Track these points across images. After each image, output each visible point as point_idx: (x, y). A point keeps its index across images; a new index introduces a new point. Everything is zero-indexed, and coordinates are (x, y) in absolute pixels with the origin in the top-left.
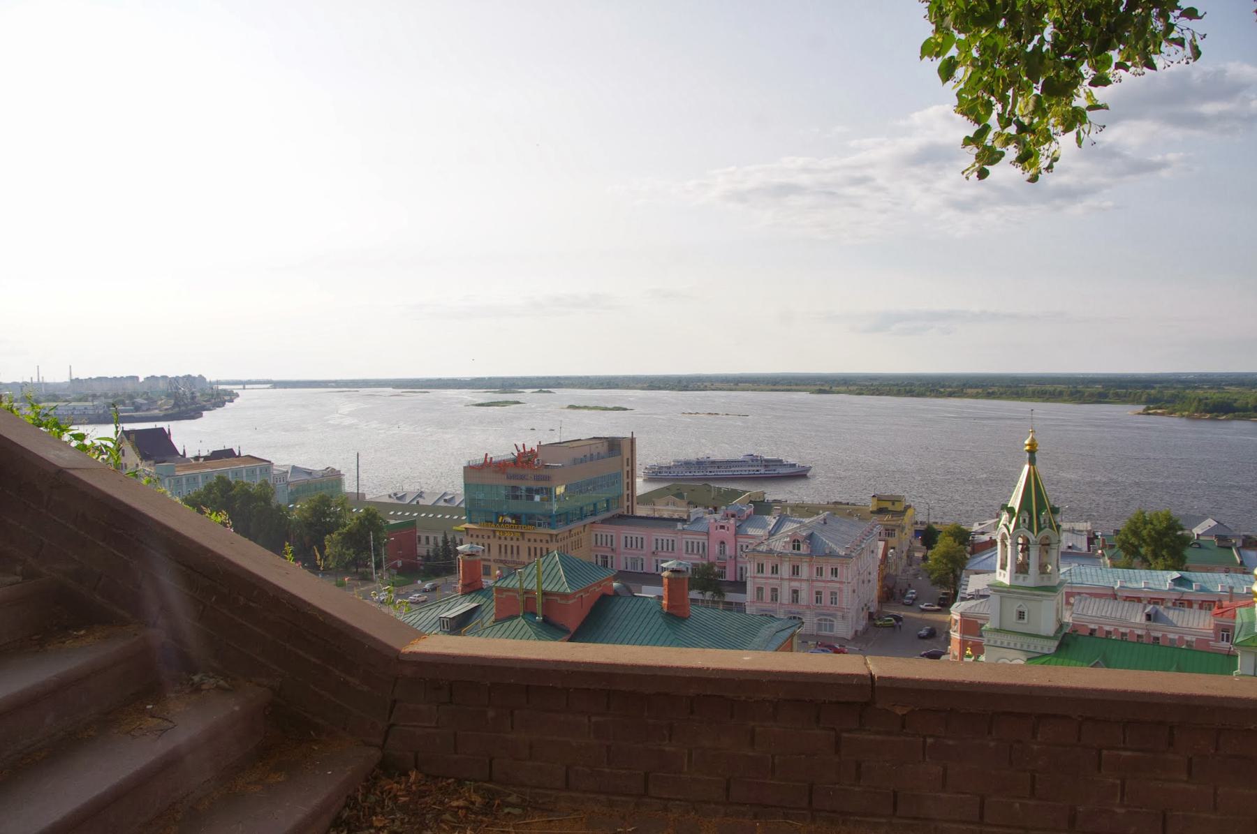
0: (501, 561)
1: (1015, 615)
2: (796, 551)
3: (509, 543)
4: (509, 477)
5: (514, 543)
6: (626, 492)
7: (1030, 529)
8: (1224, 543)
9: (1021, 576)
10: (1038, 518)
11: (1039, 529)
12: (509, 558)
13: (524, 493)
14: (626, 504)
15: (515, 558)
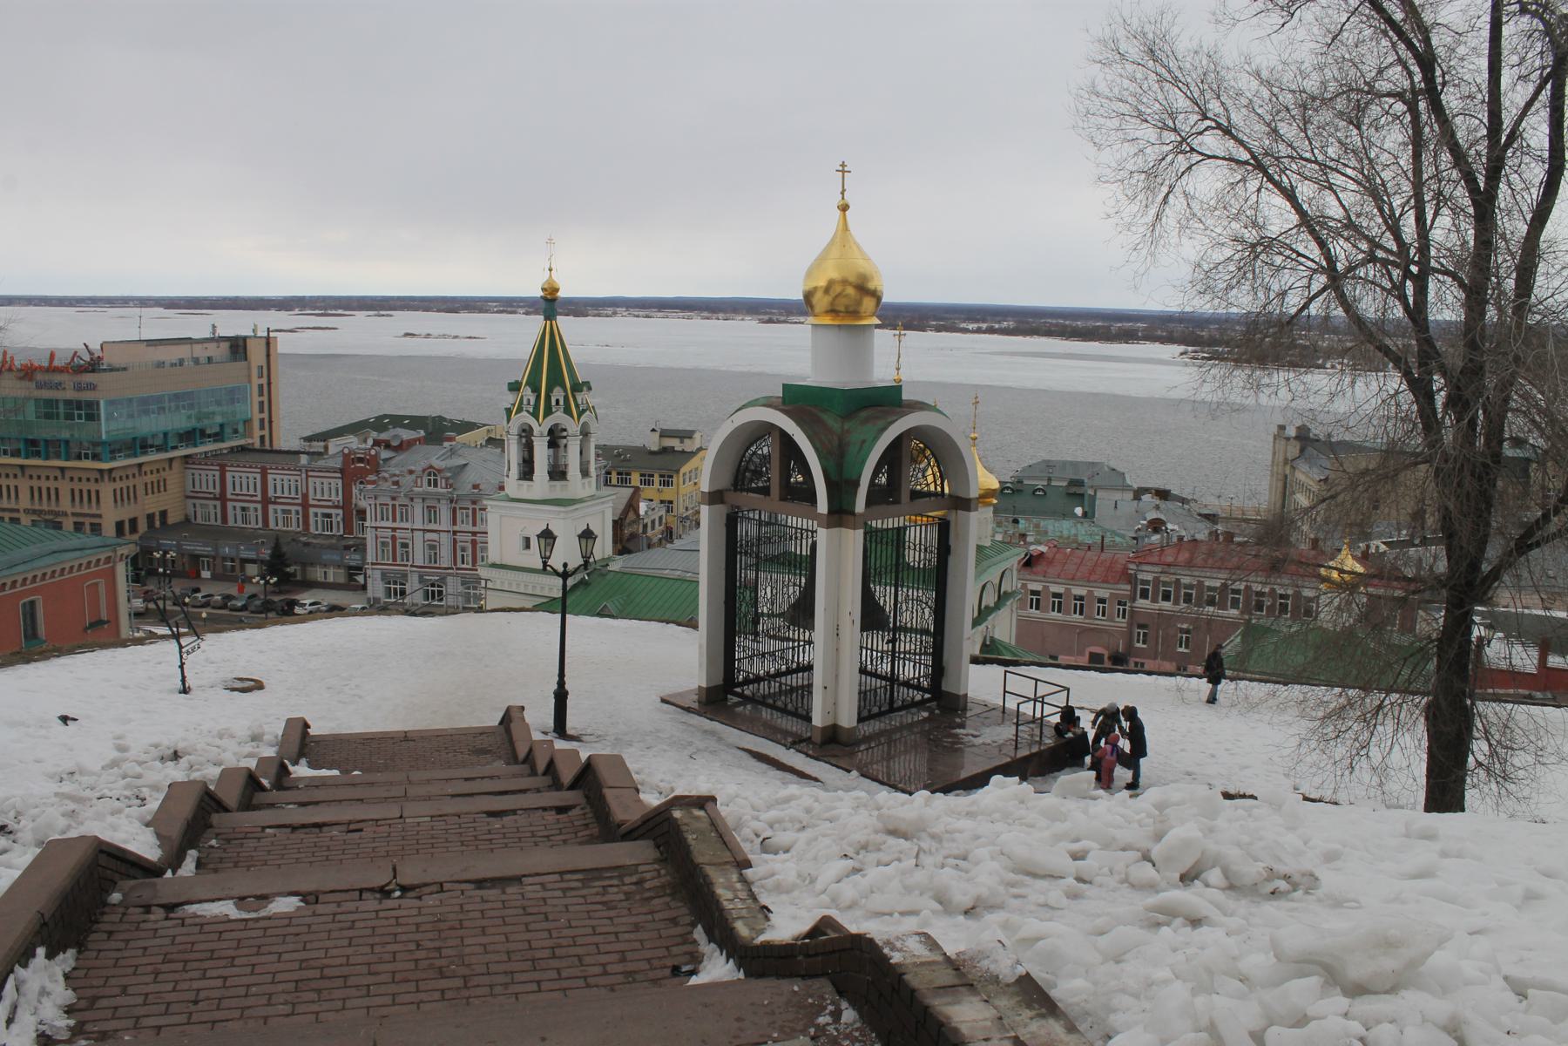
0: (34, 512)
1: (520, 543)
2: (431, 489)
3: (44, 484)
4: (39, 386)
5: (52, 484)
6: (257, 417)
7: (535, 415)
8: (1073, 490)
9: (526, 483)
10: (548, 398)
11: (548, 412)
12: (45, 507)
13: (62, 409)
14: (257, 433)
15: (53, 507)
